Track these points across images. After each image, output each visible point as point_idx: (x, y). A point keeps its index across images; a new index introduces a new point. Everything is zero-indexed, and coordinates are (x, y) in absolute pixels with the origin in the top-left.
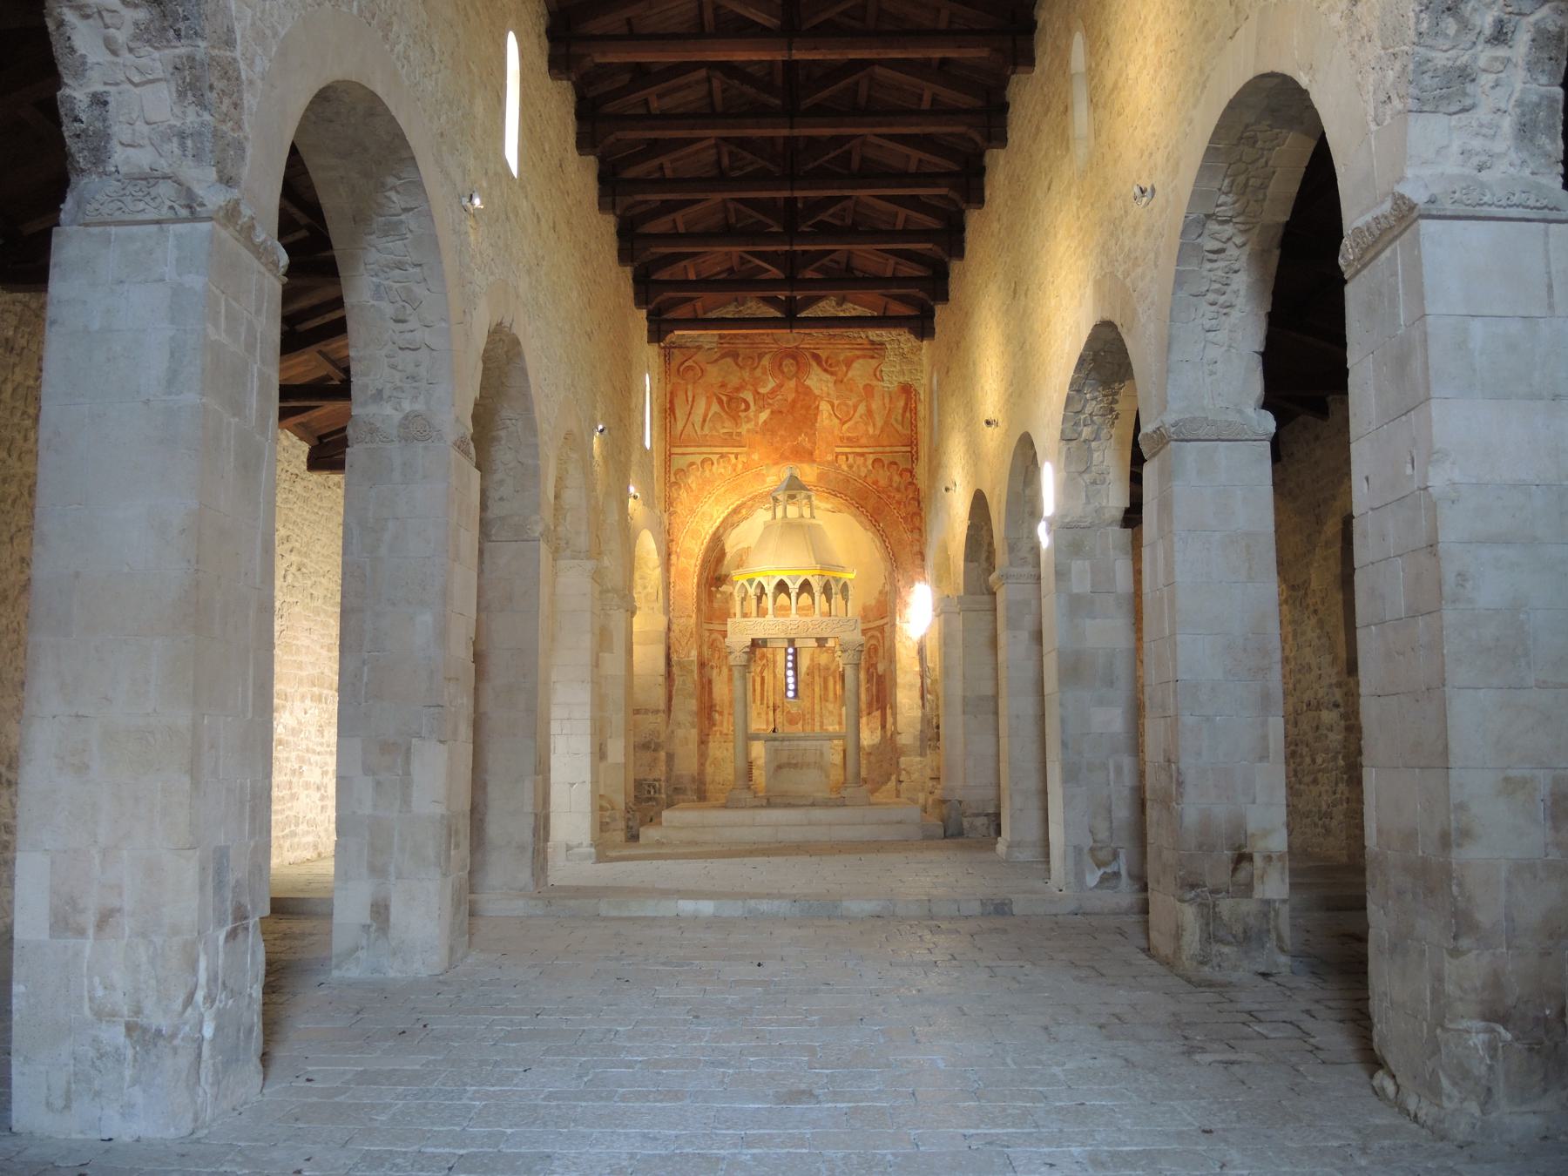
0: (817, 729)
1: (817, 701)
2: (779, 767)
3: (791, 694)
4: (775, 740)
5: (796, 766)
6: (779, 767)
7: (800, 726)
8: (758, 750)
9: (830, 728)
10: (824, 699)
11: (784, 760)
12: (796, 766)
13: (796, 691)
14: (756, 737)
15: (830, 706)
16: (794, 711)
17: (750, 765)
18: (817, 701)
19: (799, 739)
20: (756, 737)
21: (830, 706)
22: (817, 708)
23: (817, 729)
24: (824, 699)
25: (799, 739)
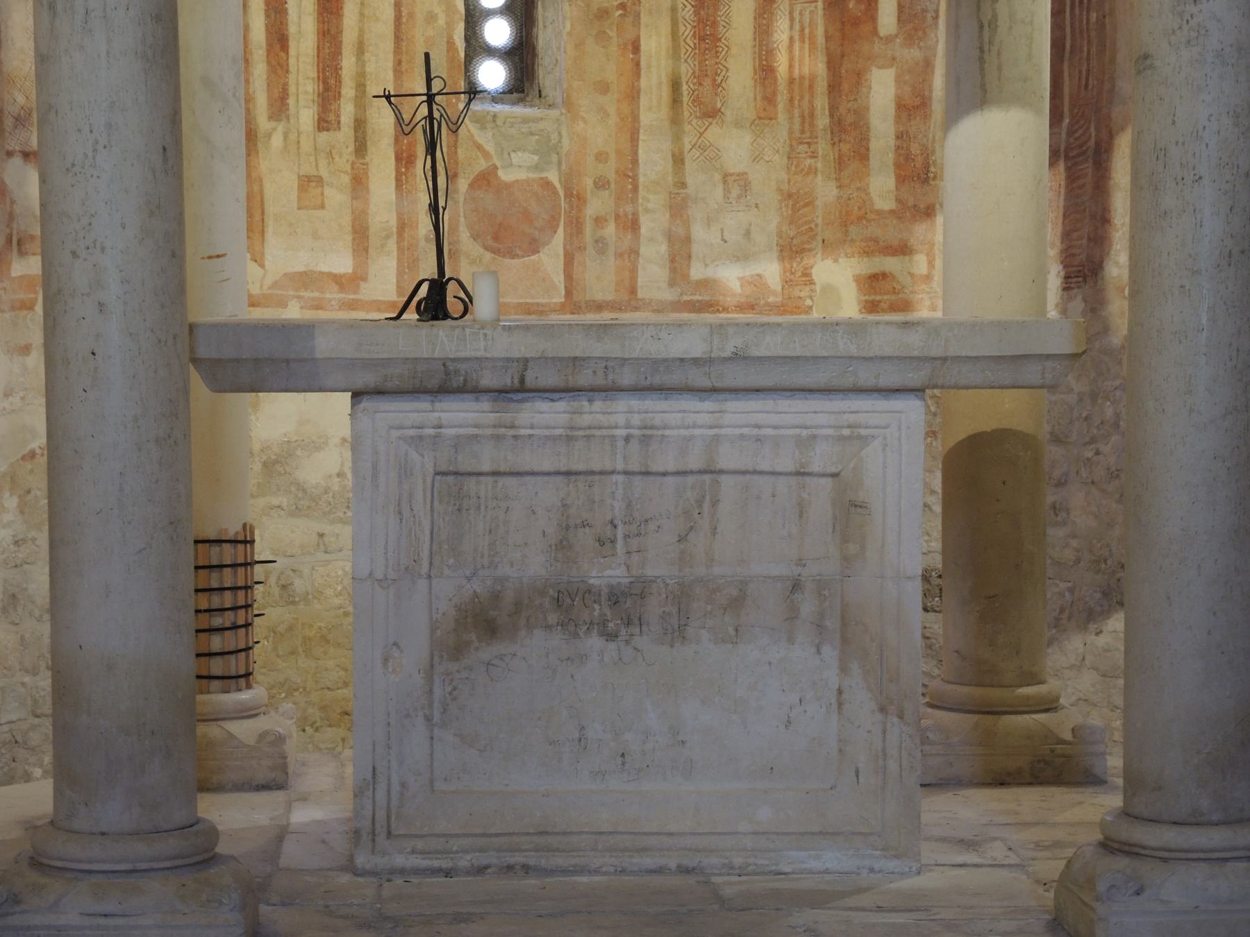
0: (653, 277)
1: (653, 112)
2: (484, 622)
3: (492, 75)
4: (446, 383)
5: (622, 610)
6: (484, 622)
7: (551, 259)
8: (300, 448)
9: (731, 278)
10: (696, 99)
11: (531, 564)
12: (622, 610)
13: (521, 57)
14: (270, 360)
15: (735, 146)
16: (517, 169)
17: (219, 585)
18: (653, 112)
19: (660, 380)
20: (270, 360)
21: (735, 146)
22: (653, 159)
23: (653, 277)
24: (696, 99)
25: (660, 380)
